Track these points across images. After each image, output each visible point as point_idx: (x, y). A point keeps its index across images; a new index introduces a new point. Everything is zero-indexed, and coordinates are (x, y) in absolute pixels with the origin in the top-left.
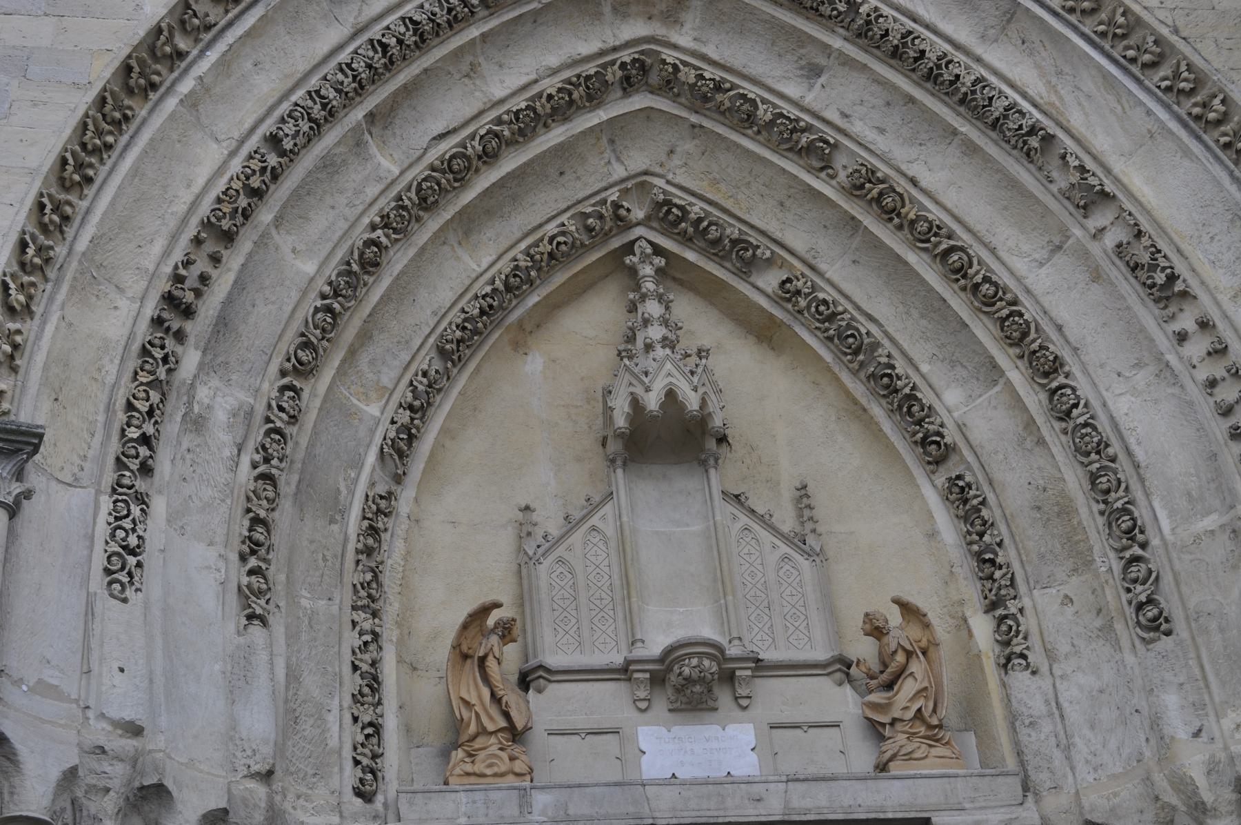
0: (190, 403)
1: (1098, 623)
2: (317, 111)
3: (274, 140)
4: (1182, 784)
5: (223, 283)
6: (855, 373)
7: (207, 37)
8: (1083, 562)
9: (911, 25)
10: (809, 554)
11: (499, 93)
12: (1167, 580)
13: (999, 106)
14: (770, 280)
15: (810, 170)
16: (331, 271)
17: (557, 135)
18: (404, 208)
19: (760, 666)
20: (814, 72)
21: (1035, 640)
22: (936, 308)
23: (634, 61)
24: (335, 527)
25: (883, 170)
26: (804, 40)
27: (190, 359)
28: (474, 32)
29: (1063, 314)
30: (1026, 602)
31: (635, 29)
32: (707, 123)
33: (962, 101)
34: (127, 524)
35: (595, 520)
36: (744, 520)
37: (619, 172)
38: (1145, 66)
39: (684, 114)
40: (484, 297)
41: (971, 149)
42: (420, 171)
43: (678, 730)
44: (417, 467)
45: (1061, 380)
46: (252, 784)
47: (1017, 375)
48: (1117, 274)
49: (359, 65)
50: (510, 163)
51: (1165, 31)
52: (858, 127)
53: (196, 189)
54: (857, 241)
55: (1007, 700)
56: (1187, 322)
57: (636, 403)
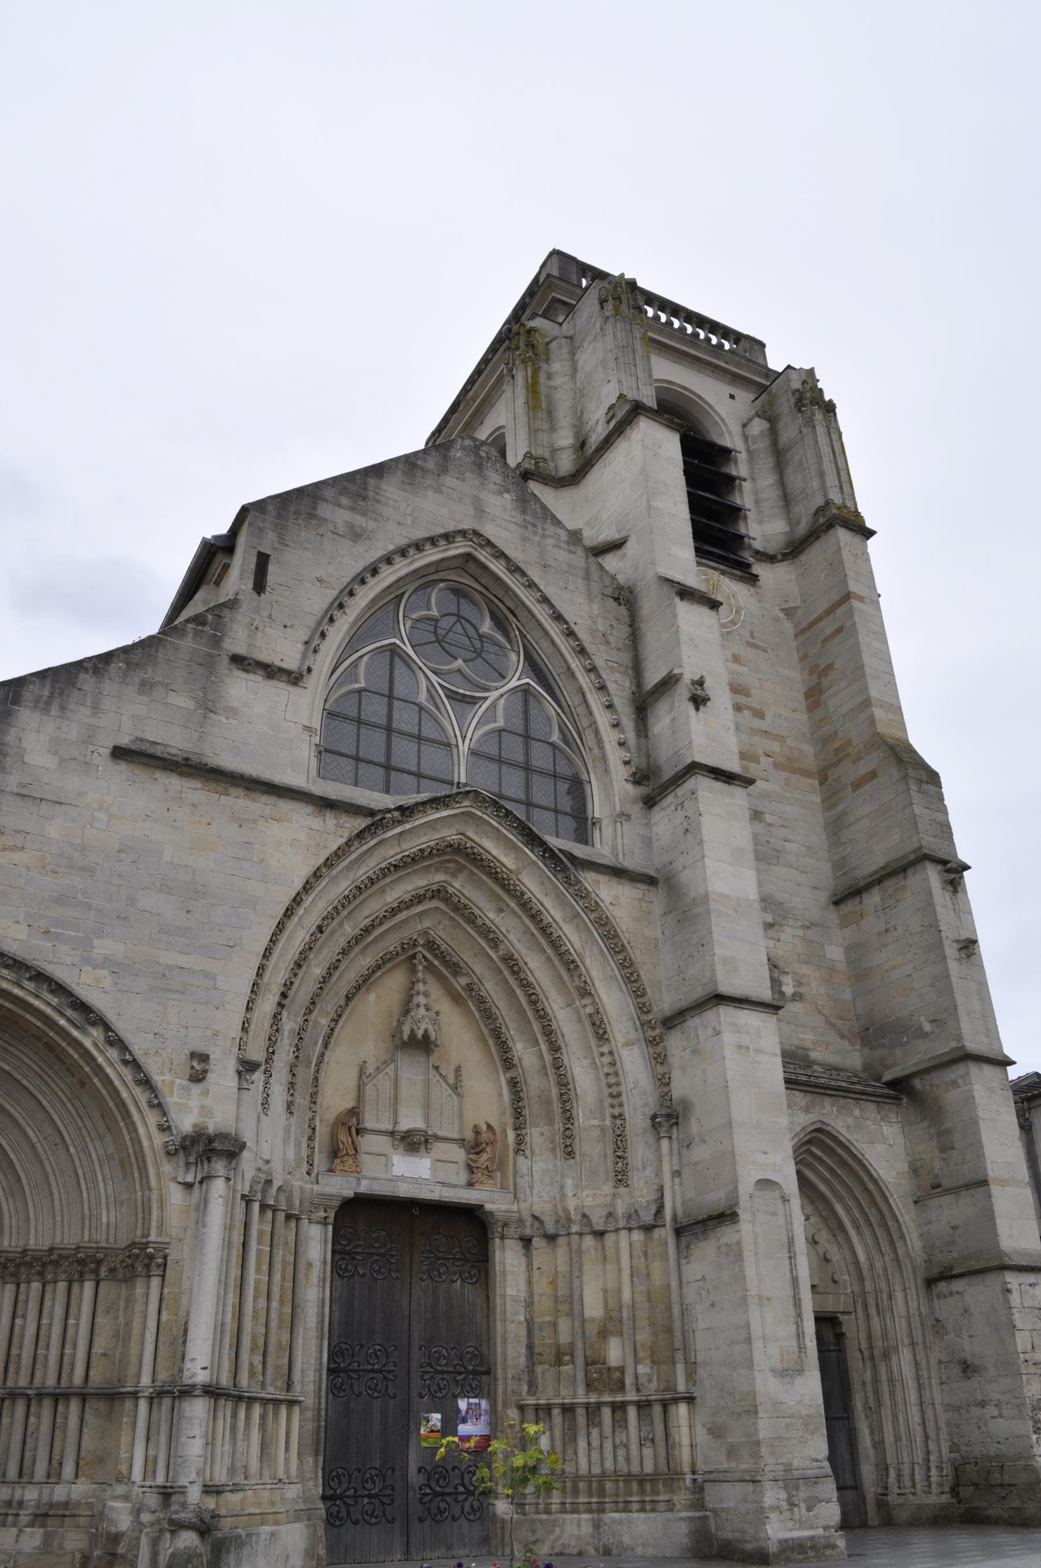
1: (551, 1146)
4: (566, 1210)
6: (486, 1025)
8: (551, 1122)
10: (458, 1095)
12: (577, 1139)
13: (564, 948)
14: (464, 981)
15: (490, 946)
19: (438, 1138)
20: (501, 910)
21: (529, 1145)
22: (523, 1013)
25: (516, 956)
26: (501, 899)
29: (565, 1030)
30: (528, 1131)
31: (440, 877)
32: (457, 918)
33: (551, 942)
35: (387, 1070)
36: (438, 1077)
37: (419, 927)
38: (615, 952)
39: (449, 912)
41: (549, 959)
43: (407, 1158)
45: (558, 1055)
47: (544, 1047)
48: (587, 1023)
51: (625, 942)
52: (511, 937)
54: (500, 977)
55: (515, 1165)
56: (605, 1049)
57: (412, 1030)
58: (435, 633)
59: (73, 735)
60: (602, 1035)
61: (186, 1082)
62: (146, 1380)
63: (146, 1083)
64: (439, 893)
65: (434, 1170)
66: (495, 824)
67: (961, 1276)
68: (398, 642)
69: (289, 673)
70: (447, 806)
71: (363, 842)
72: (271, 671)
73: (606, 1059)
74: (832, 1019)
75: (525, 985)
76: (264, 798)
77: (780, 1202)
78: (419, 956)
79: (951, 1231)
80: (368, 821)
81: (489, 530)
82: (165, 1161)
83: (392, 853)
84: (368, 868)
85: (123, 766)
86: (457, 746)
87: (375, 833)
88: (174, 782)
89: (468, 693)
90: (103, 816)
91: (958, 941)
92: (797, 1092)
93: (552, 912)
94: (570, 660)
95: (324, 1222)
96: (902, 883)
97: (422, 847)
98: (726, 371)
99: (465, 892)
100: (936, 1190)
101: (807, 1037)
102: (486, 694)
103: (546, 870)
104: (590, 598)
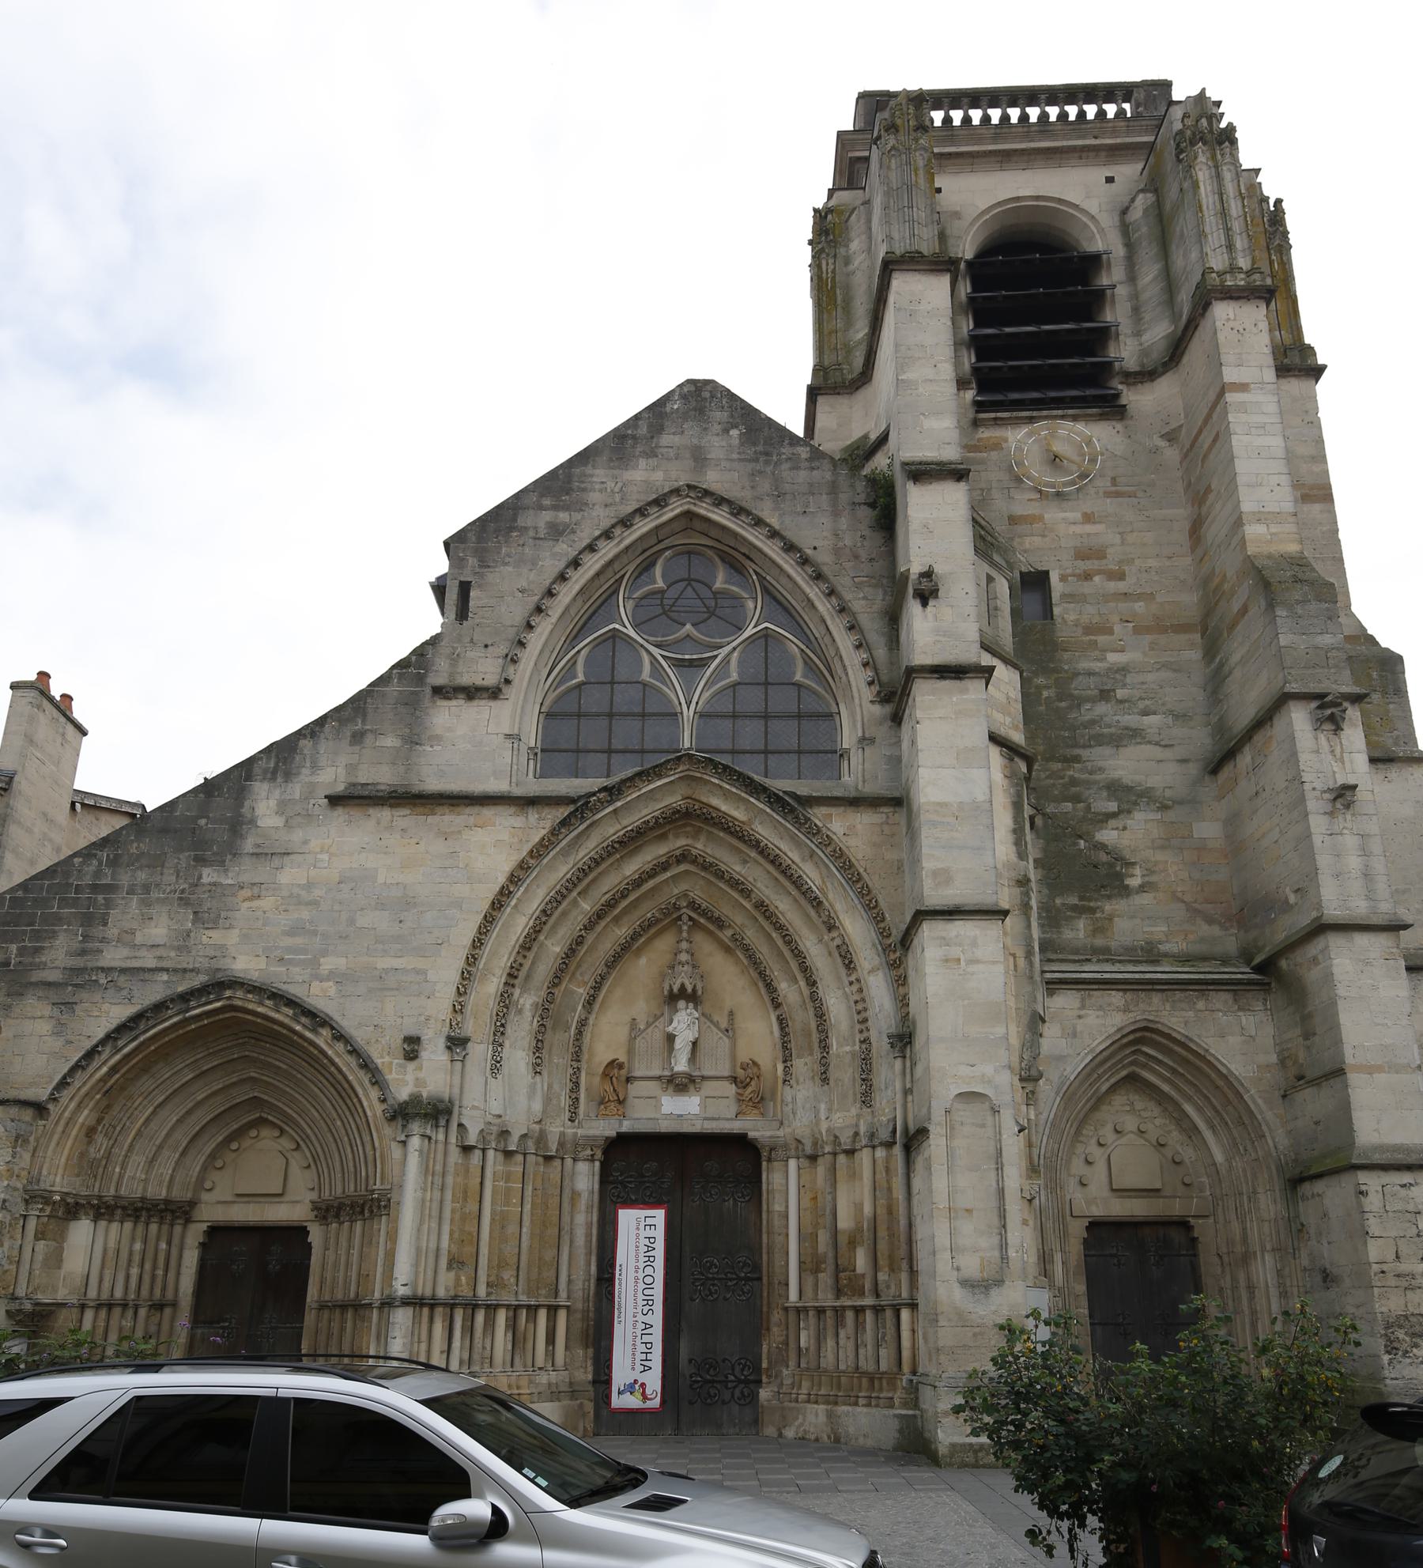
2: (559, 898)
3: (544, 911)
5: (527, 964)
9: (778, 852)
11: (628, 874)
14: (729, 933)
17: (651, 883)
22: (781, 954)
25: (767, 902)
26: (741, 851)
31: (682, 842)
37: (676, 891)
41: (796, 900)
47: (802, 983)
49: (574, 879)
52: (759, 885)
58: (662, 604)
59: (297, 796)
60: (849, 965)
61: (402, 1061)
62: (377, 1295)
63: (366, 1065)
64: (683, 857)
66: (716, 781)
67: (1320, 1176)
68: (617, 626)
69: (485, 689)
70: (660, 776)
71: (572, 828)
72: (471, 693)
73: (855, 988)
74: (1196, 906)
75: (779, 927)
76: (468, 810)
77: (989, 1113)
78: (685, 918)
79: (1314, 1126)
80: (572, 808)
81: (713, 479)
82: (386, 1125)
83: (612, 831)
84: (588, 850)
85: (340, 811)
86: (682, 713)
87: (583, 817)
88: (385, 814)
90: (325, 857)
91: (1330, 790)
92: (1113, 992)
93: (790, 854)
94: (808, 590)
96: (1269, 734)
98: (1096, 149)
99: (709, 851)
100: (1301, 1082)
101: (1158, 929)
103: (775, 815)
104: (836, 514)
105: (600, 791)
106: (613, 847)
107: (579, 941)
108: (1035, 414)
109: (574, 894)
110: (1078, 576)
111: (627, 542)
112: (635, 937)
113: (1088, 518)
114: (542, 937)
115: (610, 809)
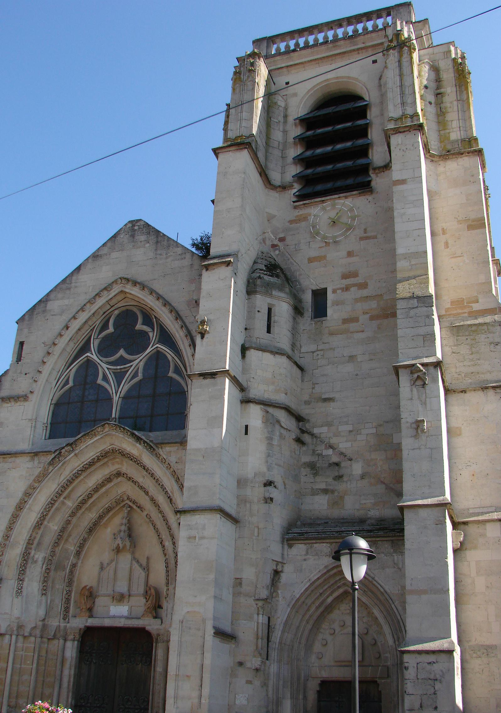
0: (33, 559)
2: (52, 502)
7: (30, 496)
14: (145, 513)
16: (60, 527)
17: (104, 489)
18: (74, 512)
23: (116, 473)
24: (64, 572)
27: (33, 552)
28: (82, 477)
34: (19, 585)
40: (94, 522)
42: (76, 504)
44: (82, 556)
46: (40, 622)
50: (96, 496)
53: (32, 523)
65: (130, 611)
74: (391, 485)
75: (161, 512)
80: (53, 456)
83: (77, 465)
89: (122, 367)
92: (324, 544)
95: (74, 640)
97: (93, 457)
101: (368, 501)
102: (131, 364)
105: (67, 445)
106: (78, 473)
107: (68, 522)
108: (323, 199)
109: (62, 498)
110: (342, 289)
111: (92, 312)
112: (101, 517)
113: (350, 254)
114: (46, 522)
115: (73, 454)
